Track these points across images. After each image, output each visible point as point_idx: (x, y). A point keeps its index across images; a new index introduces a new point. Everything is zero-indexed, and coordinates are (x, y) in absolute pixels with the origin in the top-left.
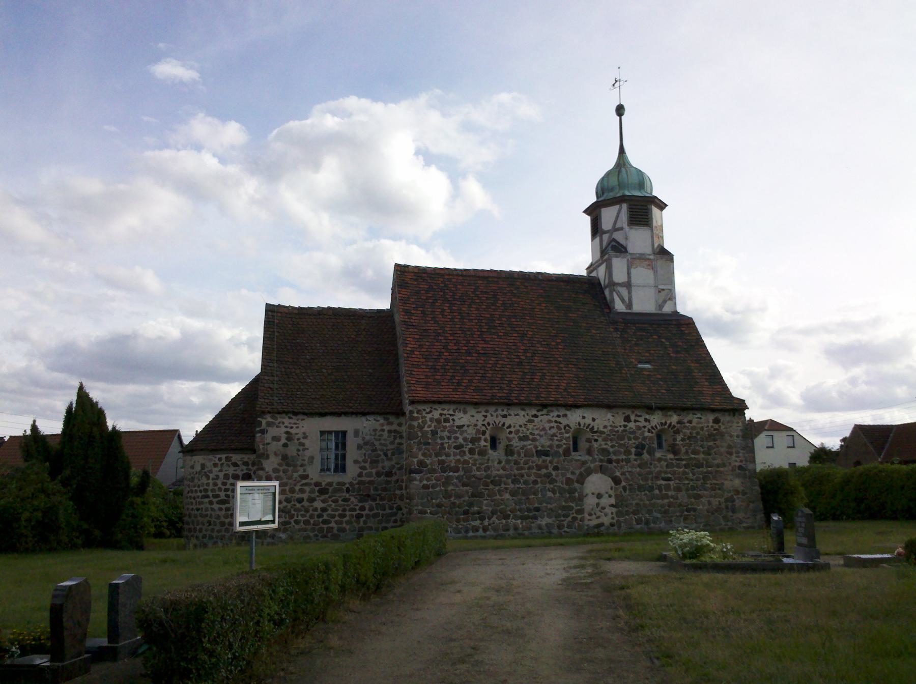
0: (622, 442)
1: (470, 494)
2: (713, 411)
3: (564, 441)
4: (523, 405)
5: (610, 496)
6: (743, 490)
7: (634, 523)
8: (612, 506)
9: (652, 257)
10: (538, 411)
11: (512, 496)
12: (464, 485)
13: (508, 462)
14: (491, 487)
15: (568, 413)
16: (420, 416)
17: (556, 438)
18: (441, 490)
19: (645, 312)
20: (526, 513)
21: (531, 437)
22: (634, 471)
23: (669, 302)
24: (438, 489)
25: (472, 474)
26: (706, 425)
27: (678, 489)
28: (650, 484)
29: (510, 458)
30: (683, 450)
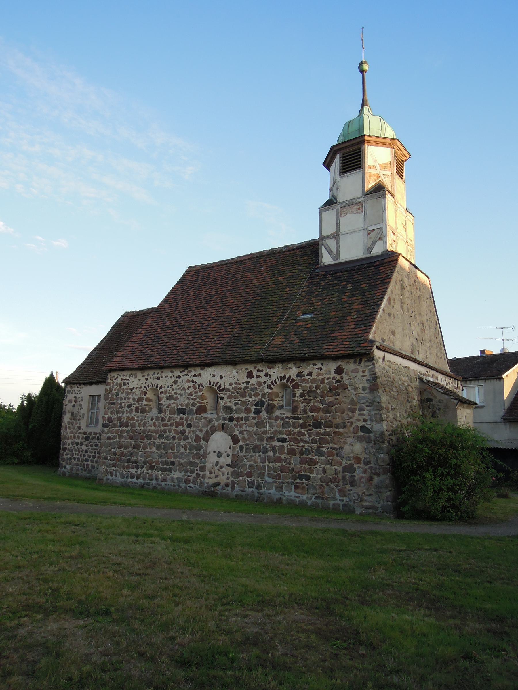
0: (244, 400)
1: (132, 445)
2: (335, 358)
3: (198, 400)
4: (171, 367)
5: (228, 455)
6: (366, 458)
7: (247, 485)
8: (228, 465)
9: (362, 200)
10: (181, 372)
11: (157, 450)
12: (131, 438)
13: (157, 418)
14: (146, 440)
15: (202, 372)
16: (112, 381)
17: (191, 397)
18: (117, 441)
19: (352, 259)
20: (165, 466)
21: (174, 396)
22: (250, 430)
23: (379, 244)
24: (115, 440)
25: (135, 429)
26: (327, 376)
27: (291, 452)
28: (265, 445)
29: (159, 415)
30: (301, 406)
